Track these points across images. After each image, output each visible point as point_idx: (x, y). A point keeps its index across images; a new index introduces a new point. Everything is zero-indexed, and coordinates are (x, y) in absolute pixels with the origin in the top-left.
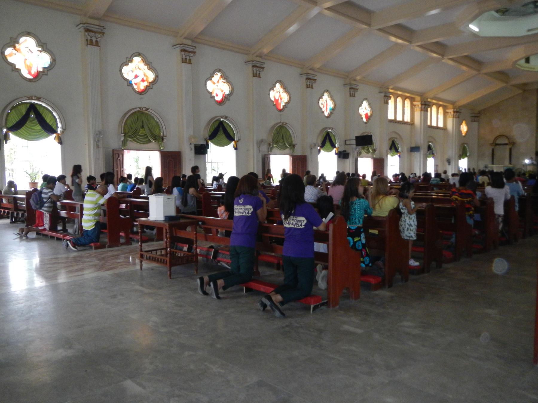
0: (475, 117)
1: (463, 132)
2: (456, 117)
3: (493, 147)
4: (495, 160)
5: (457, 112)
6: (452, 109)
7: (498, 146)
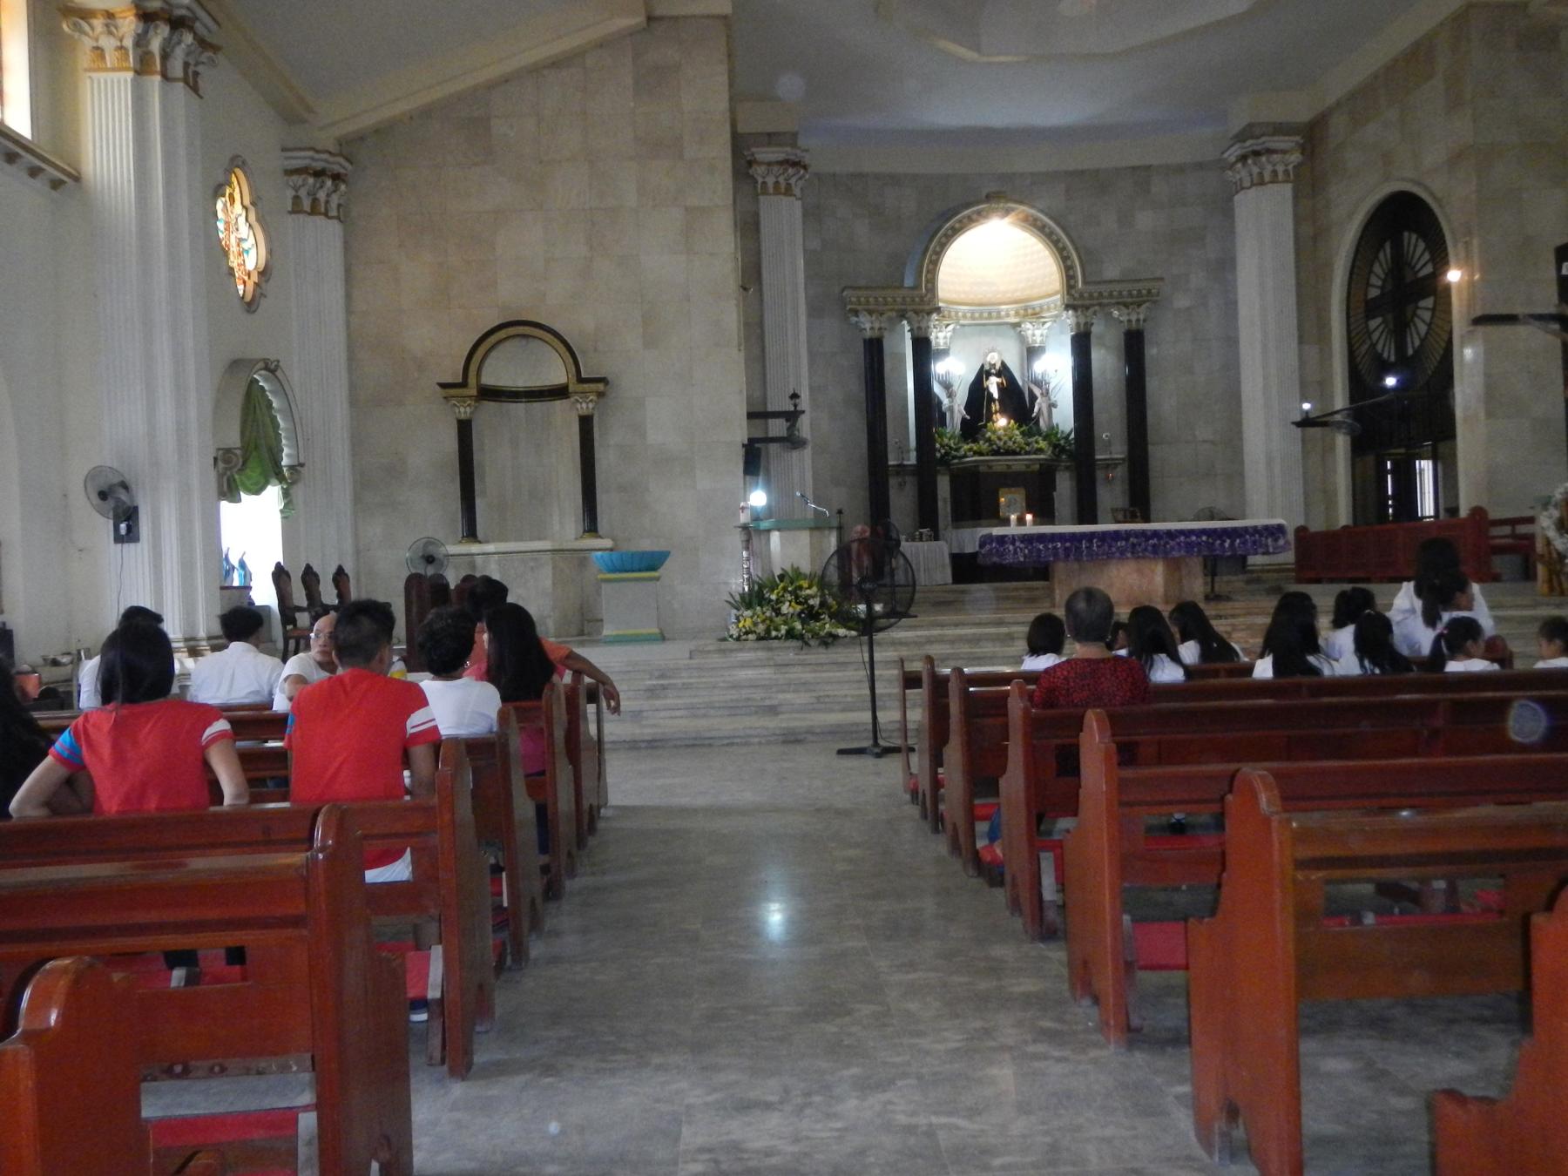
0: (318, 174)
1: (234, 261)
2: (165, 77)
3: (464, 411)
4: (480, 504)
5: (178, 24)
7: (490, 406)
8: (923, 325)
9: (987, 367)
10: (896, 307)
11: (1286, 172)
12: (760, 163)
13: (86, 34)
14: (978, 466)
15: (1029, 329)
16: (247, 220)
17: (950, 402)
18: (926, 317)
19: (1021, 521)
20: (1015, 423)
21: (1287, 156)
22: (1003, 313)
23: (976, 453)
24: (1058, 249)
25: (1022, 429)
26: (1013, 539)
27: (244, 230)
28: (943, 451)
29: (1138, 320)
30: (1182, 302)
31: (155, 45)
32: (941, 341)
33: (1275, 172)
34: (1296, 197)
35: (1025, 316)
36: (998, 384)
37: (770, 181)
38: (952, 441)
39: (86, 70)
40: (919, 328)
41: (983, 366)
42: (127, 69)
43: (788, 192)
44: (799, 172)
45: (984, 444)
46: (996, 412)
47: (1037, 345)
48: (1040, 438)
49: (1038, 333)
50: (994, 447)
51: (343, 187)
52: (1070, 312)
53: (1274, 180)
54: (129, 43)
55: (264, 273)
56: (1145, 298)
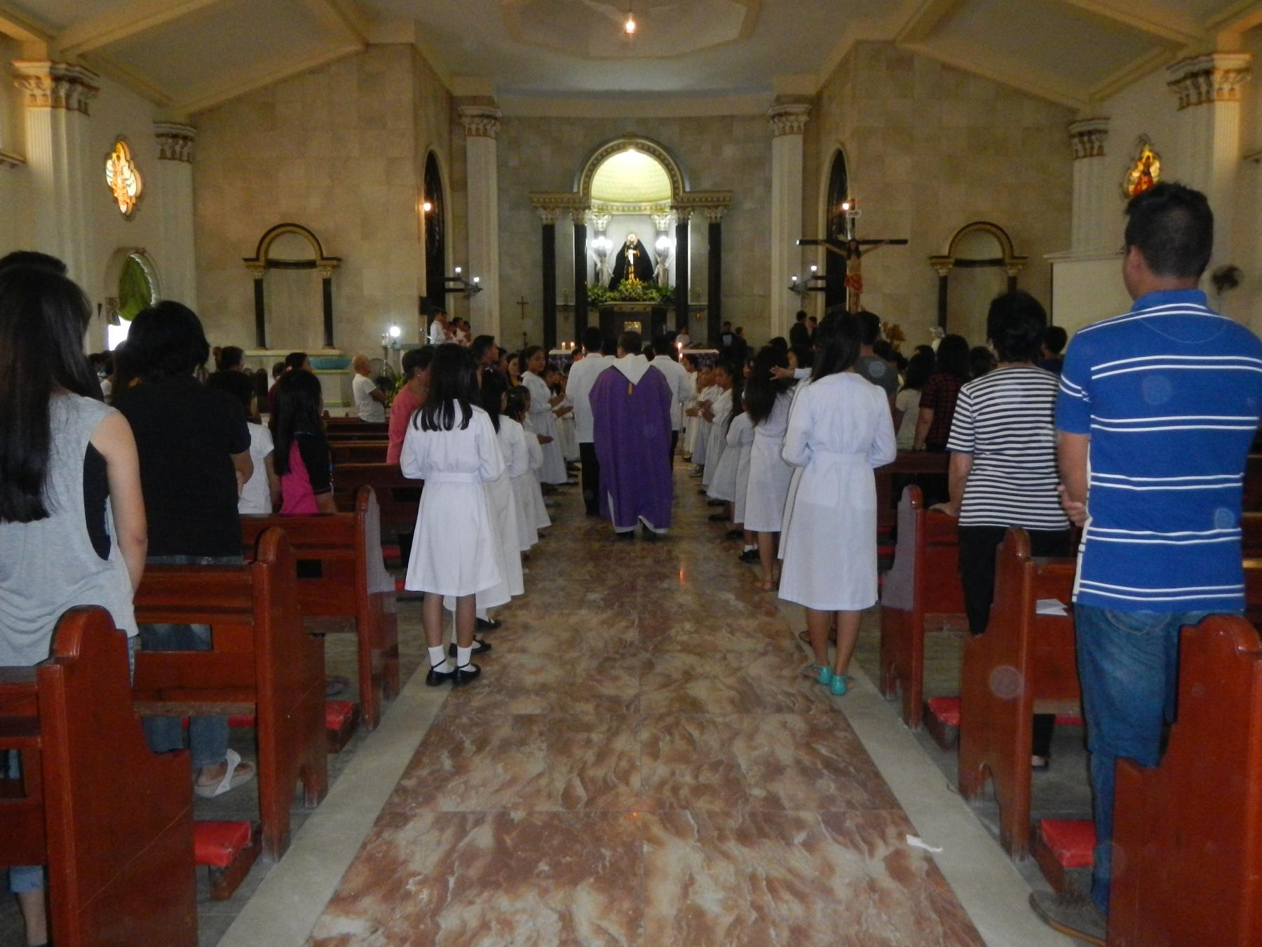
1: (119, 194)
2: (68, 108)
3: (258, 274)
5: (73, 81)
6: (40, 60)
8: (580, 217)
9: (628, 244)
10: (562, 205)
11: (799, 127)
12: (467, 116)
13: (26, 87)
14: (612, 308)
16: (129, 167)
17: (602, 266)
18: (582, 211)
19: (568, 347)
20: (640, 280)
21: (800, 117)
22: (643, 208)
23: (614, 299)
26: (561, 357)
27: (127, 173)
28: (593, 297)
29: (716, 218)
30: (748, 205)
31: (62, 93)
32: (600, 226)
33: (792, 127)
34: (805, 141)
35: (656, 209)
36: (634, 254)
37: (474, 127)
39: (29, 106)
40: (578, 219)
41: (625, 243)
42: (46, 106)
43: (485, 134)
44: (490, 122)
46: (631, 273)
47: (662, 230)
48: (655, 291)
49: (662, 222)
50: (623, 296)
51: (190, 143)
52: (674, 211)
53: (792, 131)
54: (48, 92)
55: (140, 198)
56: (722, 203)
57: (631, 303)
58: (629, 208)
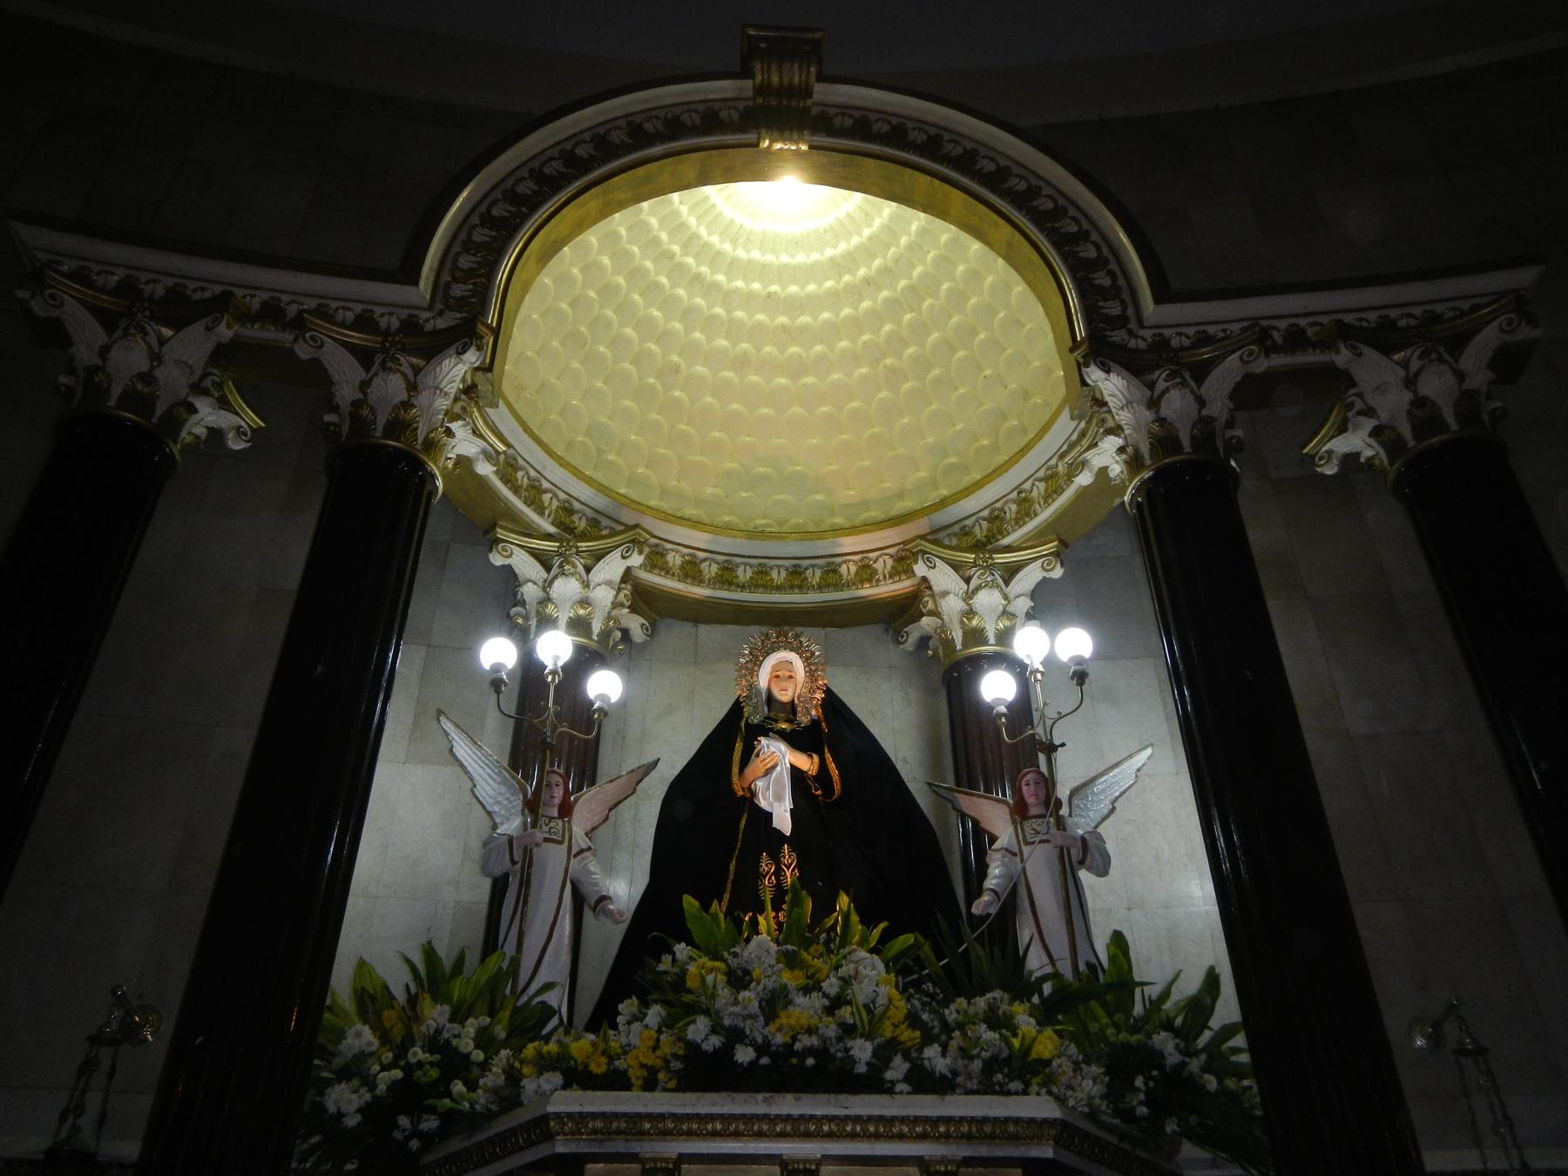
15: (945, 594)
22: (848, 570)
24: (1038, 218)
25: (906, 940)
38: (471, 1026)
41: (736, 709)
45: (639, 1017)
50: (698, 1029)
57: (788, 1105)
58: (762, 572)
